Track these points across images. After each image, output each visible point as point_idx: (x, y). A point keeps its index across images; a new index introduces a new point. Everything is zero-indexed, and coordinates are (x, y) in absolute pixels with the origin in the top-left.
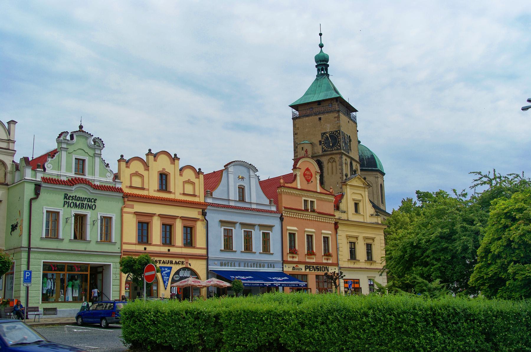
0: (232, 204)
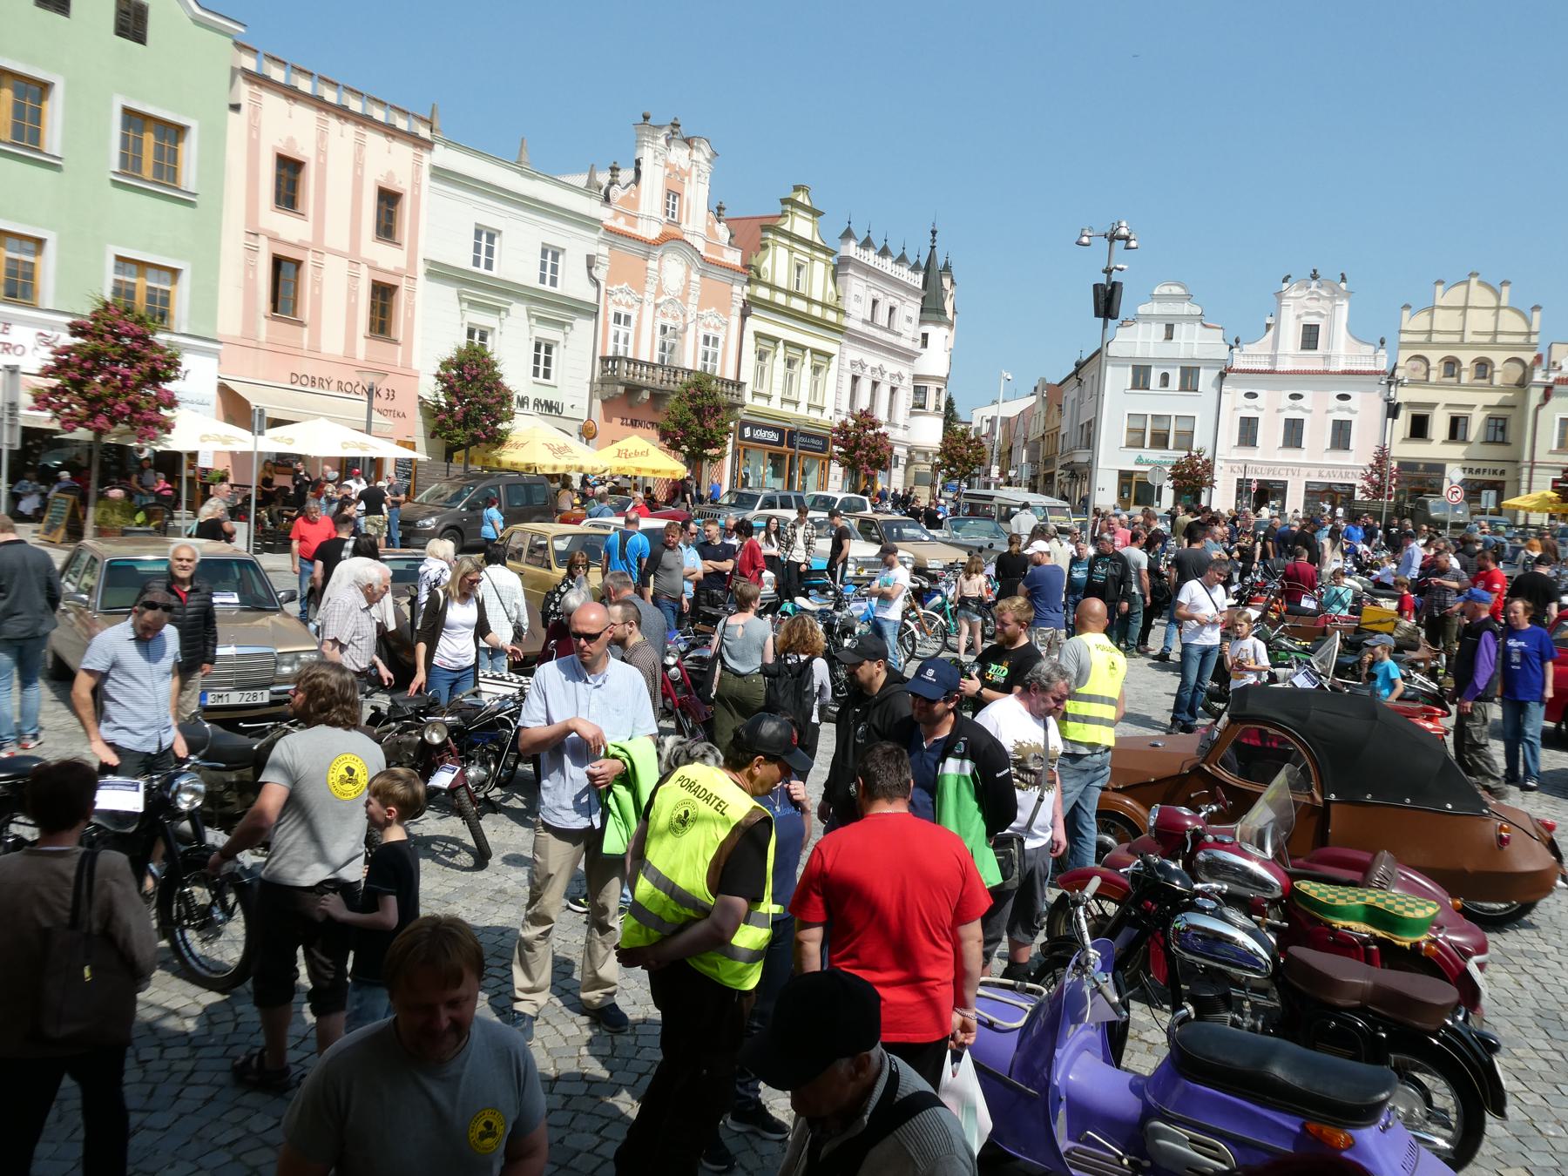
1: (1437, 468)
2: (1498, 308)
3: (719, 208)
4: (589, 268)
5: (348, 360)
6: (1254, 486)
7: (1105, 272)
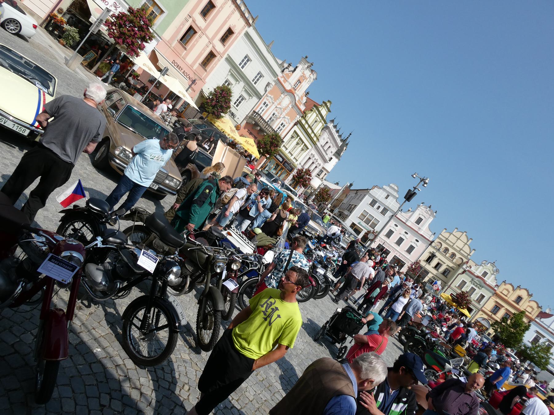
0: (549, 329)
1: (427, 272)
2: (466, 244)
3: (308, 93)
4: (267, 86)
5: (191, 67)
6: (385, 249)
7: (414, 188)
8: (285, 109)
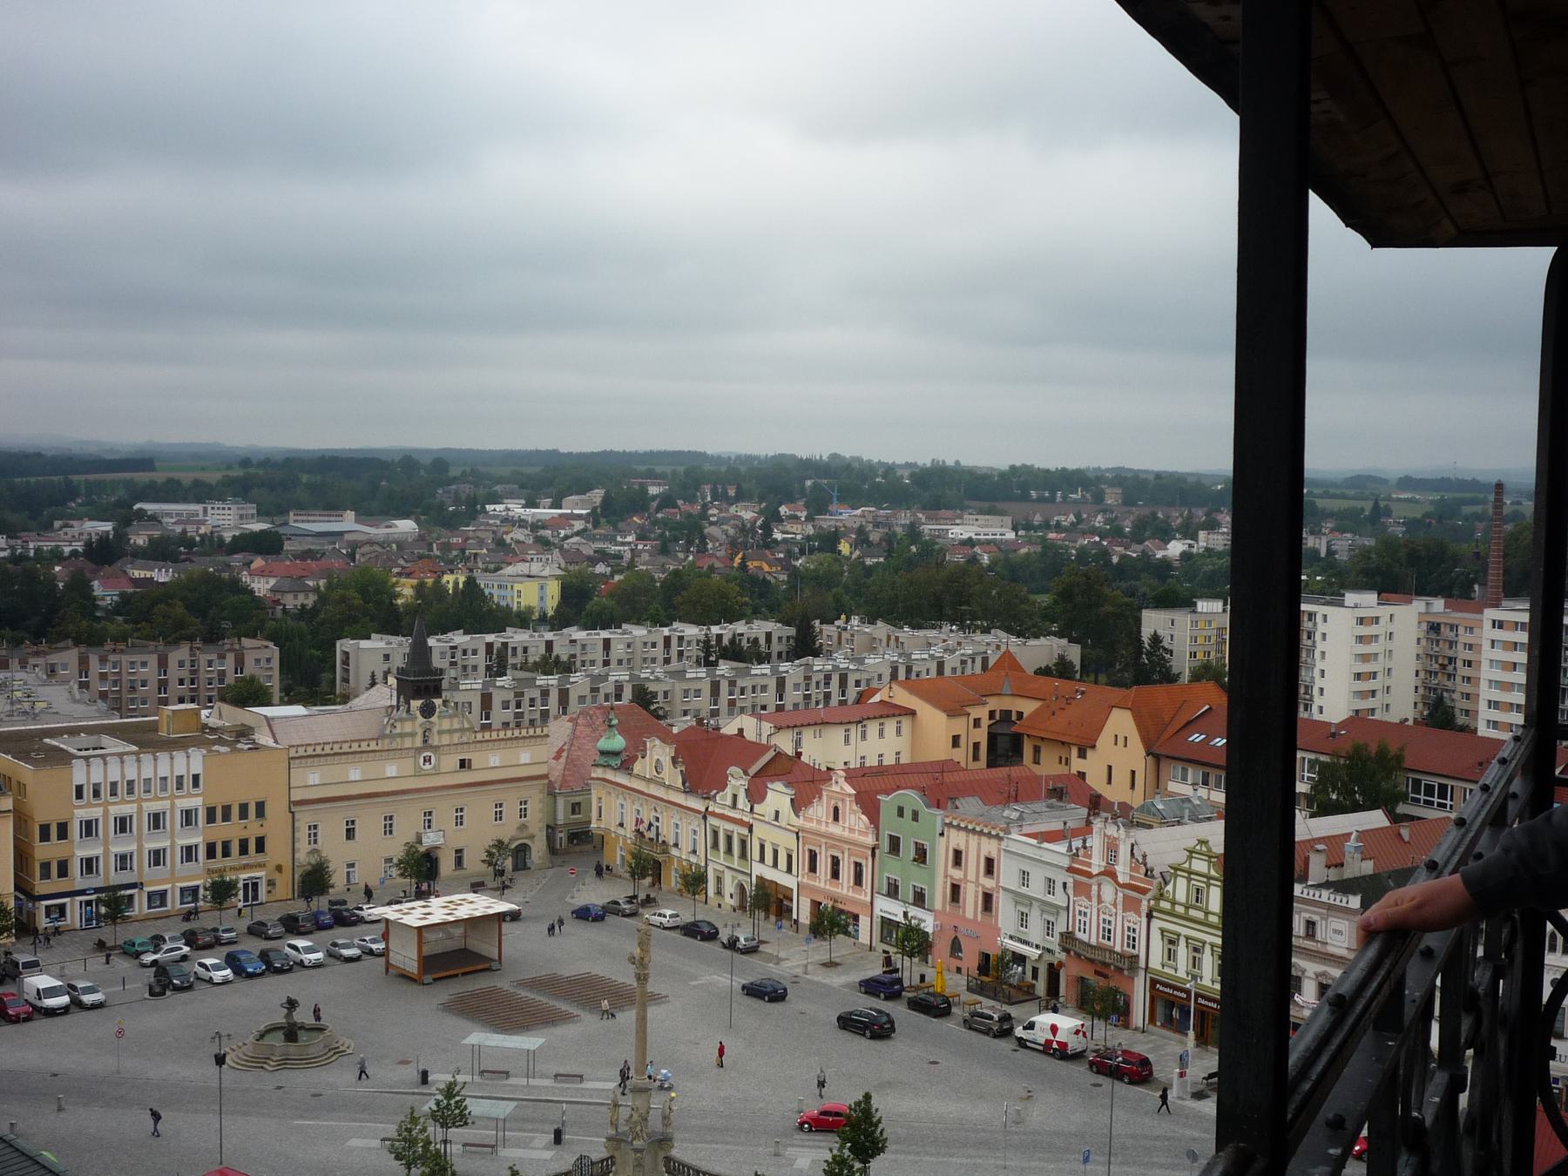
8: (1115, 905)
